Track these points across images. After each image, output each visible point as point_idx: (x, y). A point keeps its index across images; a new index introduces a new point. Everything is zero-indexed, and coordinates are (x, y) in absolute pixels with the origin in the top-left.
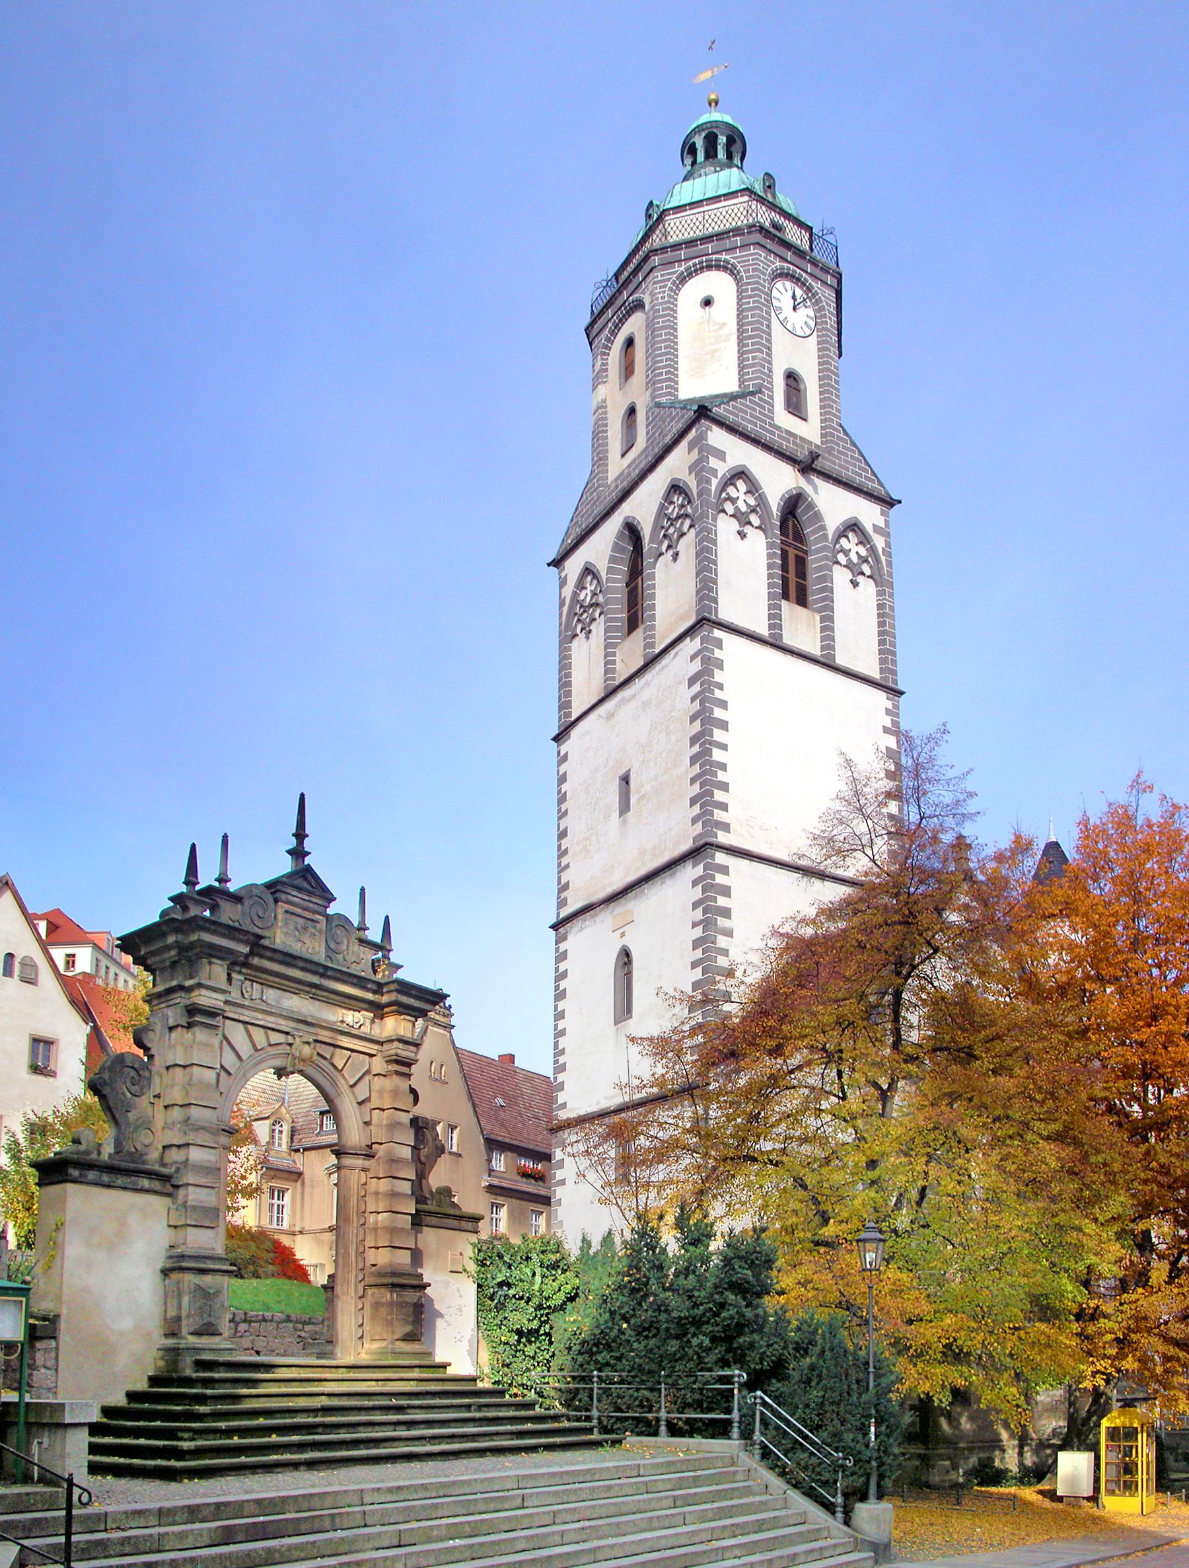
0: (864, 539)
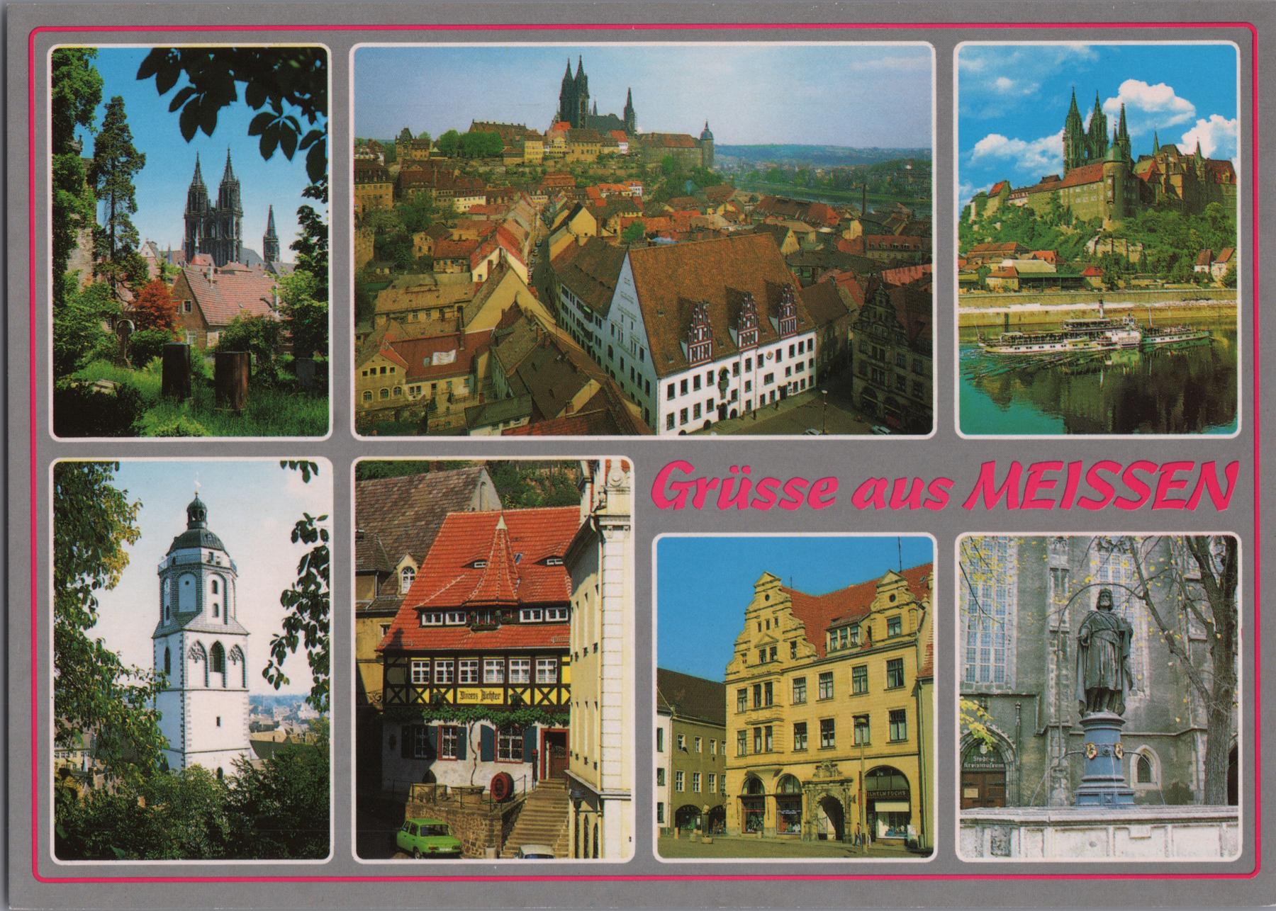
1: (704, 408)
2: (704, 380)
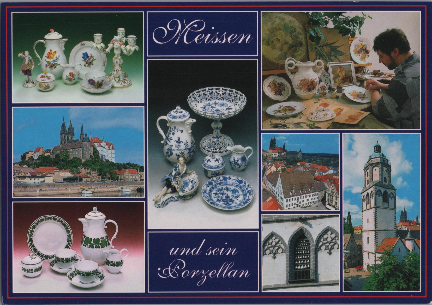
0: (393, 194)
1: (294, 204)
2: (294, 199)
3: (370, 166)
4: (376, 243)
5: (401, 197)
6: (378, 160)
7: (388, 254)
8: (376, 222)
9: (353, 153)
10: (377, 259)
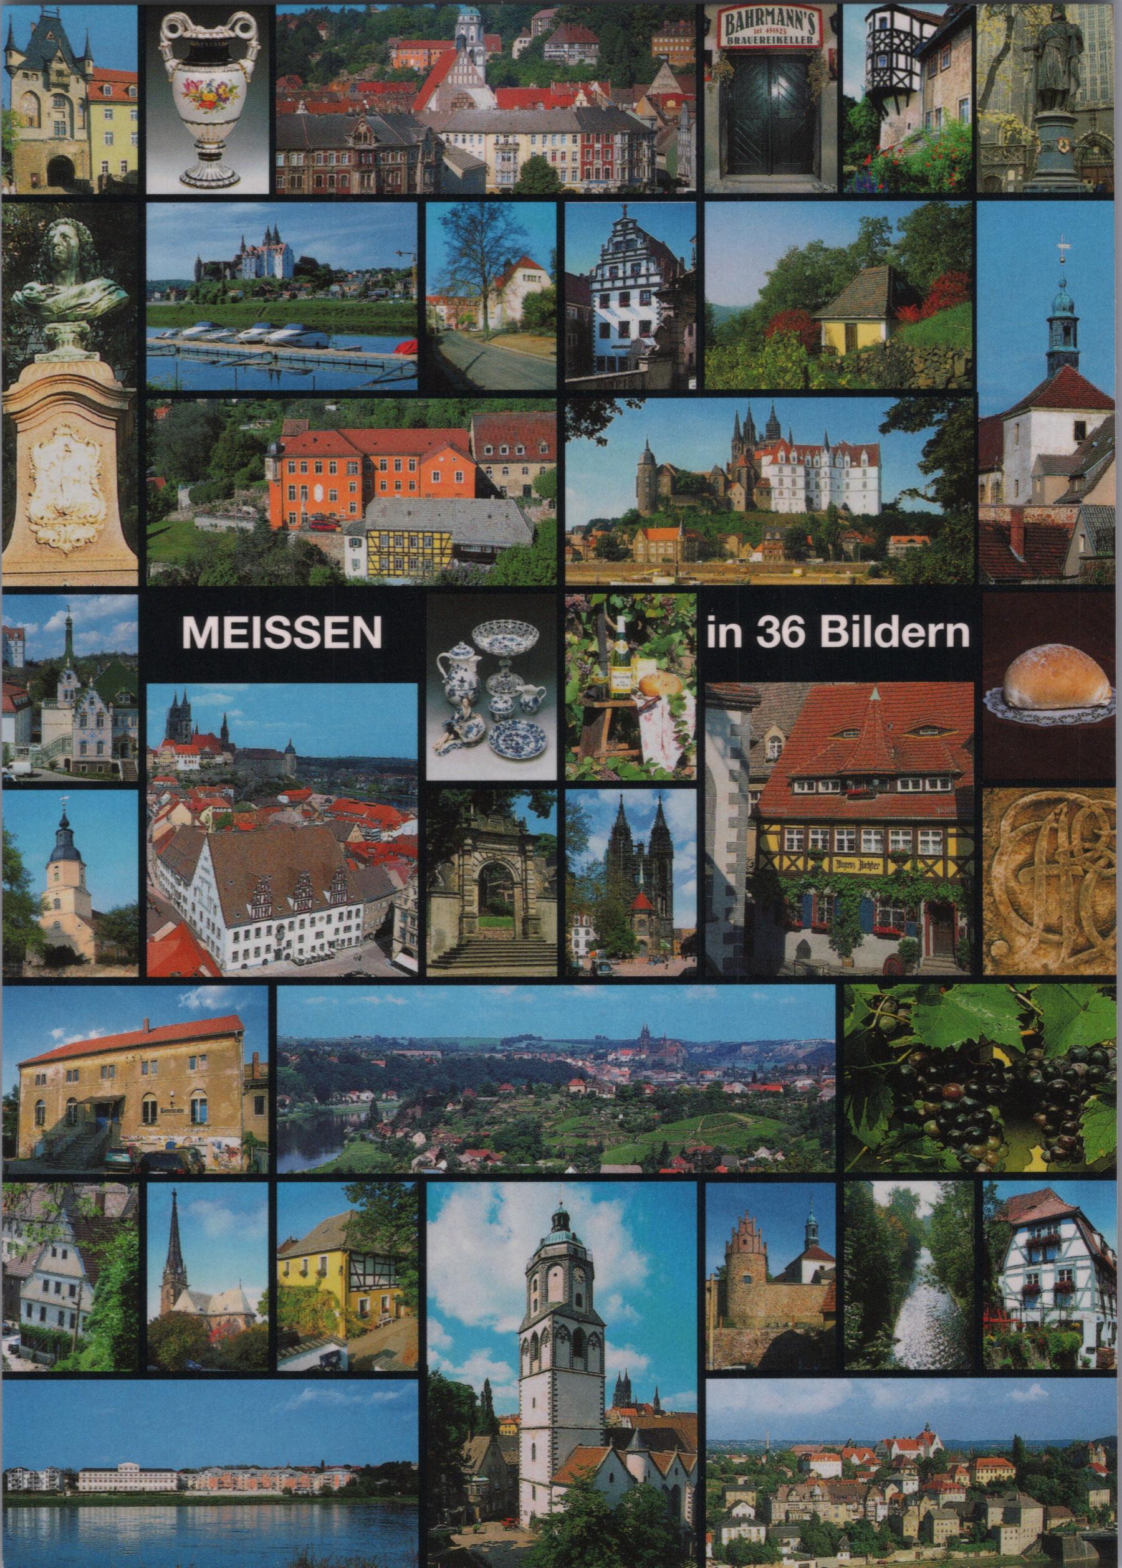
1: (263, 950)
3: (542, 1262)
4: (554, 1458)
5: (620, 1344)
6: (562, 1249)
7: (584, 1487)
8: (554, 1406)
9: (499, 1231)
10: (555, 1500)
